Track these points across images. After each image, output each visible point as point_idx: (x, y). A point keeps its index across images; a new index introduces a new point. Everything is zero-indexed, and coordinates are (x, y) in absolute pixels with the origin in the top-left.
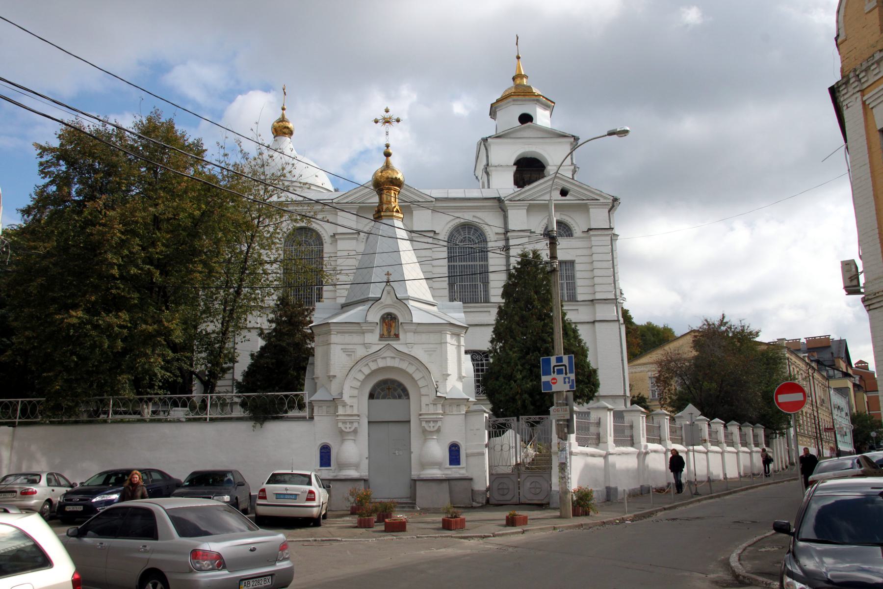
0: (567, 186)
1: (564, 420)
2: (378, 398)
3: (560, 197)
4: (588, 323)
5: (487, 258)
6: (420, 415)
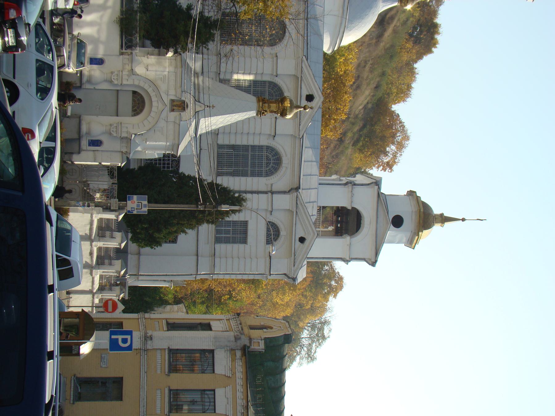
0: (307, 242)
1: (110, 206)
2: (133, 96)
3: (298, 236)
4: (197, 251)
5: (253, 176)
6: (121, 123)
